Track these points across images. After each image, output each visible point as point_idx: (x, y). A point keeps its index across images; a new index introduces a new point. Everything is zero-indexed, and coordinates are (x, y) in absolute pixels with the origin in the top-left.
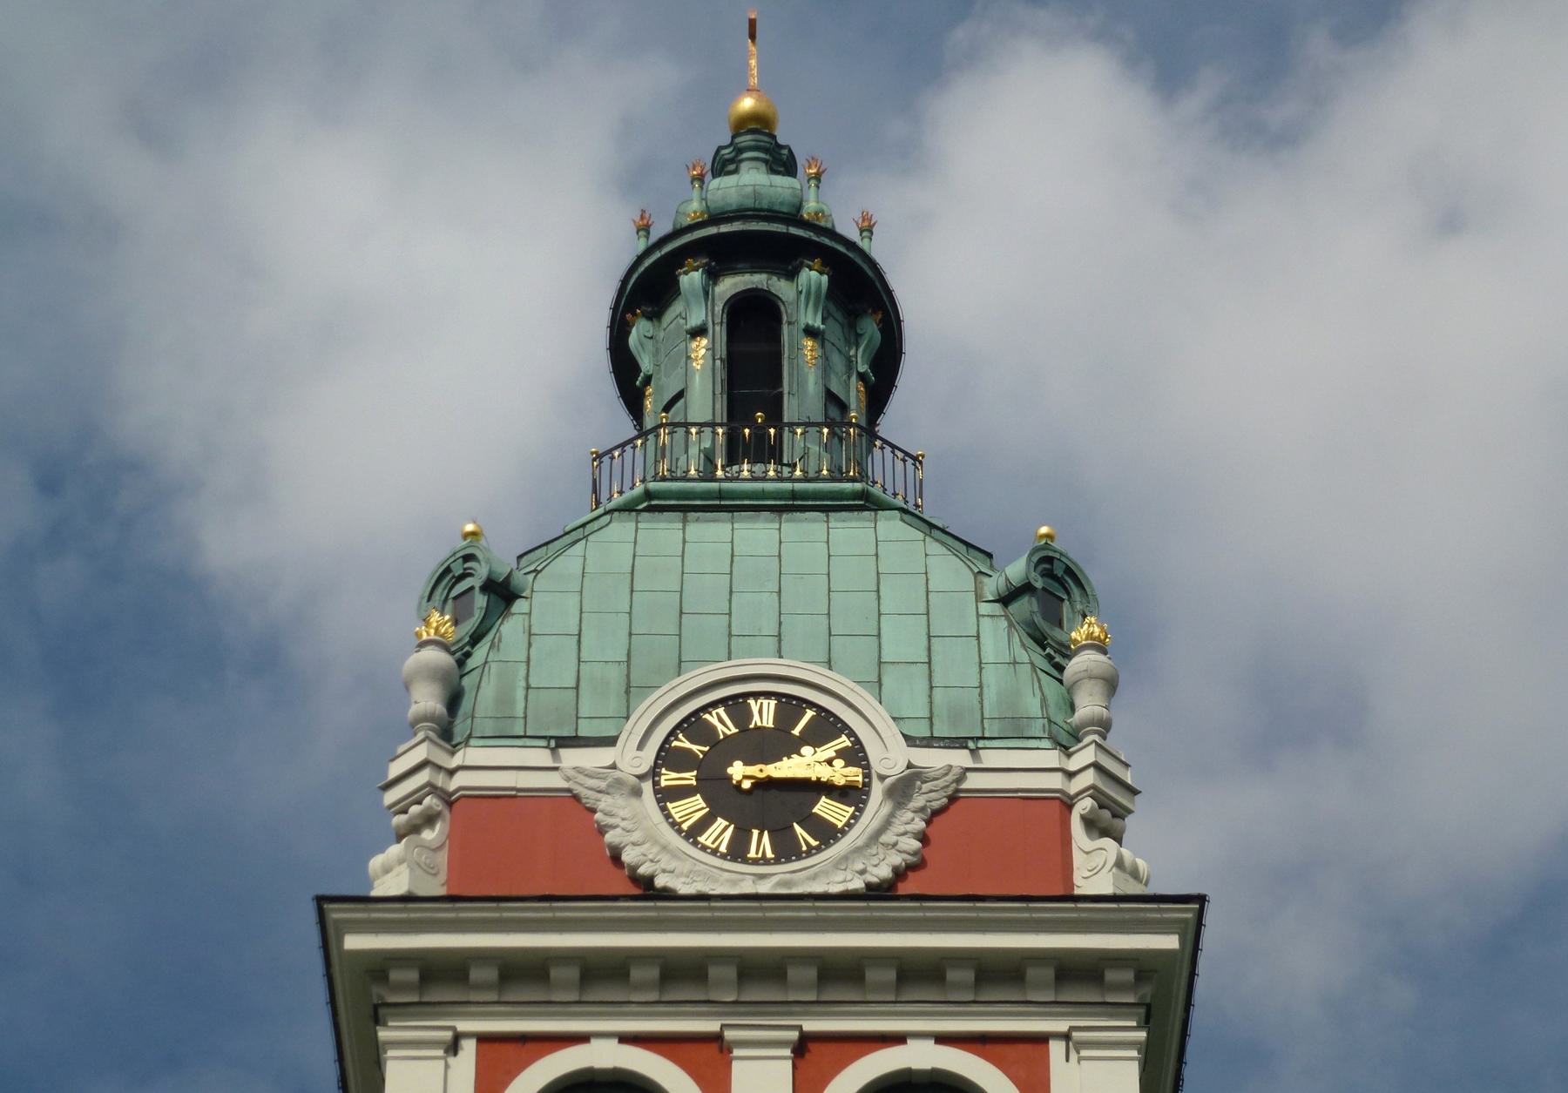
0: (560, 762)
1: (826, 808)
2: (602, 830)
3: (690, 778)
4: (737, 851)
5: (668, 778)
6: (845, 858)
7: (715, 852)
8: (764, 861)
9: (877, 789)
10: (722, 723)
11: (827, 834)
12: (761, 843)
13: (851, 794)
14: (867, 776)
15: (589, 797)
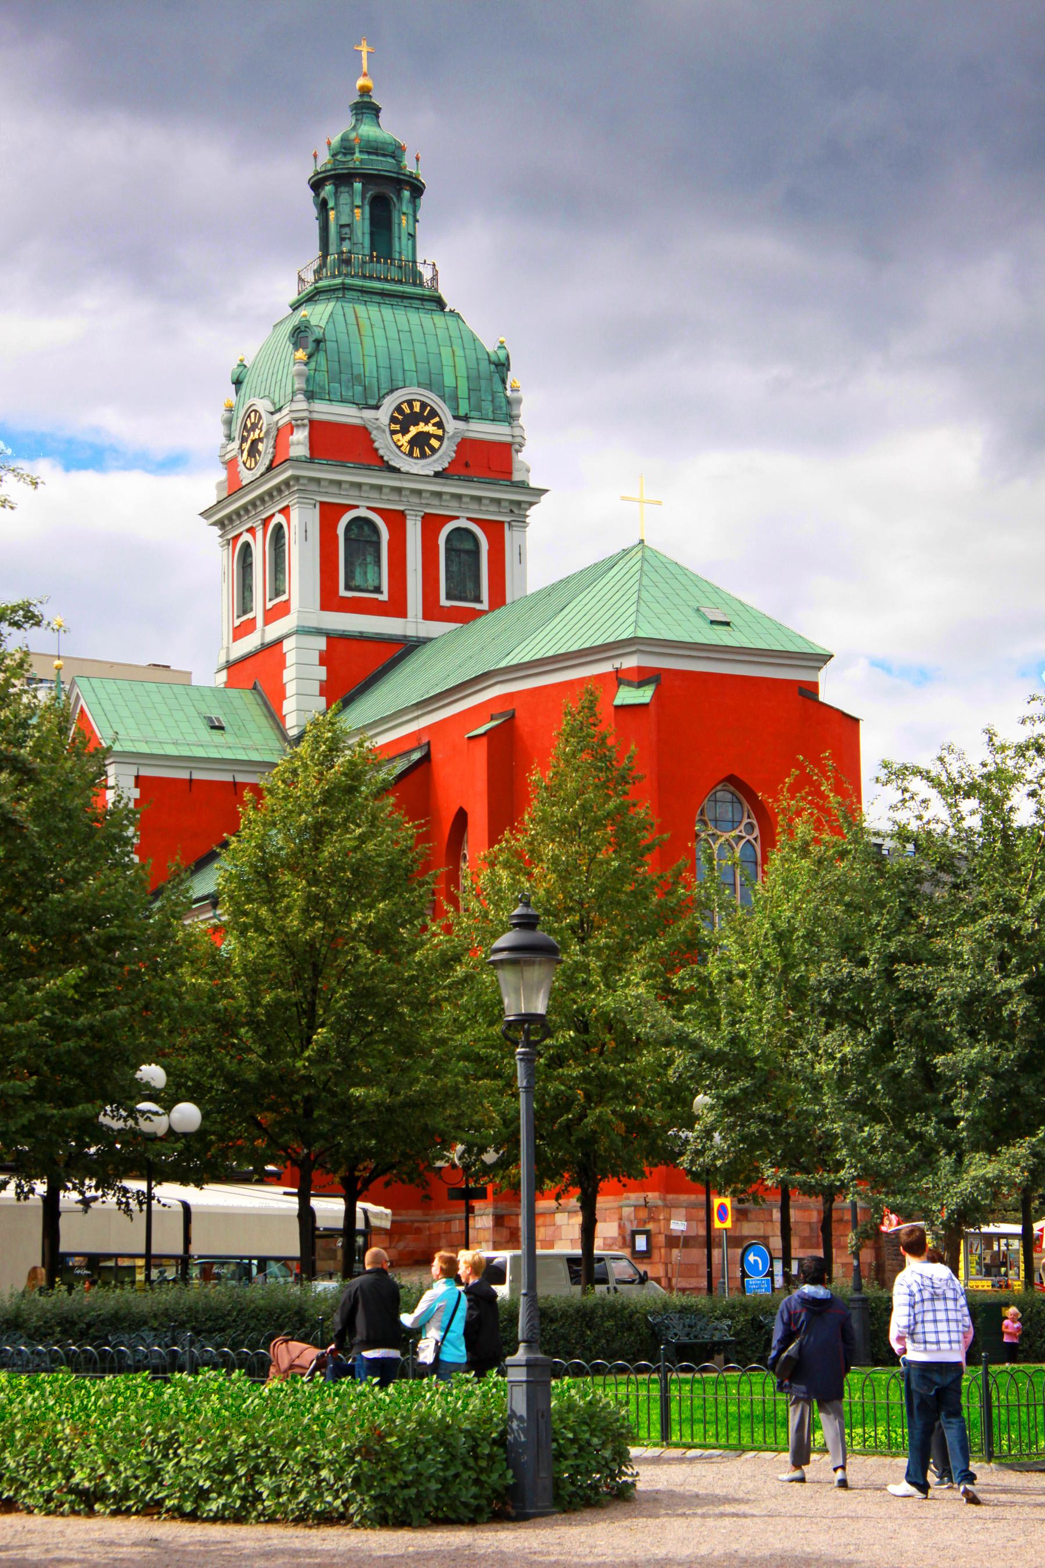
1: (434, 443)
2: (373, 442)
3: (398, 427)
4: (410, 454)
5: (394, 427)
6: (437, 460)
8: (417, 458)
9: (446, 435)
11: (434, 451)
12: (417, 452)
13: (440, 439)
14: (444, 431)
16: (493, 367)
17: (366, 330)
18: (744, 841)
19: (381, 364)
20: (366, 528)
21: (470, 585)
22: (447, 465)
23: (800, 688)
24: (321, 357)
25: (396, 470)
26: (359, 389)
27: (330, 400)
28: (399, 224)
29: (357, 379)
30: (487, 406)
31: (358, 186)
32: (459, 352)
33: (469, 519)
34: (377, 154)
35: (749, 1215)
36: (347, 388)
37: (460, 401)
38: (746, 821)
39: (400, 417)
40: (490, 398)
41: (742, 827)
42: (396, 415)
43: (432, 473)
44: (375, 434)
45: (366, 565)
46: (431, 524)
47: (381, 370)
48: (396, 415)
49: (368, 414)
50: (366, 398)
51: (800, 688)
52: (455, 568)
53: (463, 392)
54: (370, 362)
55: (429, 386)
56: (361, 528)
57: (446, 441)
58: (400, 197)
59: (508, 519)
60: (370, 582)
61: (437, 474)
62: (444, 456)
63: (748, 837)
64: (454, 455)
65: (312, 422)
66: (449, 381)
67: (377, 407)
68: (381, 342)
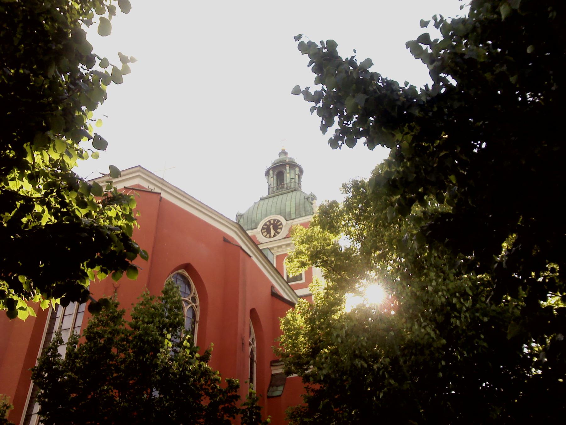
0: (85, 284)
3: (265, 230)
5: (263, 231)
10: (268, 224)
16: (306, 200)
28: (286, 177)
37: (292, 215)
49: (255, 230)
53: (293, 211)
55: (280, 214)
58: (286, 170)
66: (288, 210)
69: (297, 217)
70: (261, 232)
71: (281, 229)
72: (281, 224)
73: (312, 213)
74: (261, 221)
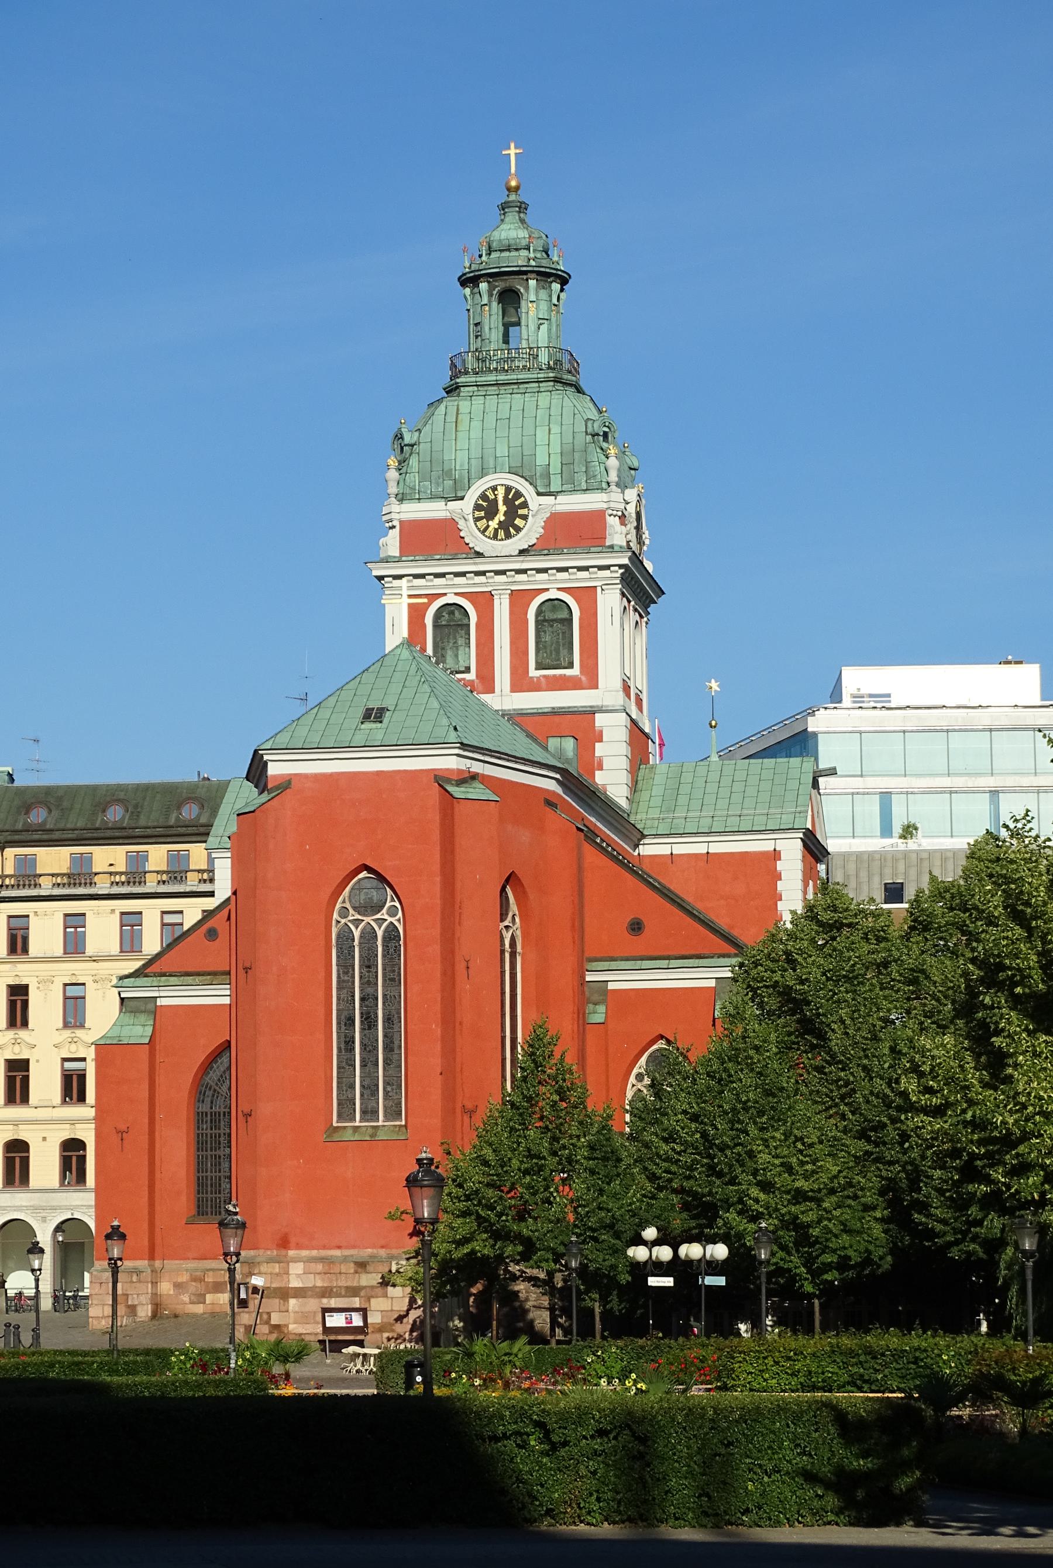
5: (477, 514)
7: (489, 538)
11: (518, 529)
13: (525, 518)
15: (457, 519)
16: (589, 437)
17: (463, 426)
18: (363, 924)
19: (473, 456)
20: (457, 613)
21: (564, 652)
22: (534, 541)
23: (436, 776)
24: (414, 461)
25: (479, 555)
26: (449, 483)
27: (419, 499)
29: (447, 474)
30: (582, 480)
31: (483, 286)
32: (556, 429)
33: (559, 589)
34: (509, 250)
35: (369, 1268)
36: (438, 484)
38: (388, 904)
39: (485, 504)
40: (584, 469)
41: (384, 911)
42: (481, 502)
43: (517, 552)
44: (461, 524)
45: (457, 648)
46: (519, 599)
47: (473, 461)
48: (481, 502)
49: (453, 505)
50: (456, 491)
51: (436, 776)
52: (547, 638)
53: (555, 467)
54: (462, 457)
56: (452, 613)
57: (530, 517)
58: (527, 288)
59: (600, 583)
60: (461, 663)
61: (522, 552)
62: (531, 531)
63: (390, 919)
64: (542, 531)
65: (401, 522)
66: (541, 460)
67: (462, 498)
68: (475, 434)
69: (565, 488)
70: (470, 518)
71: (525, 518)
72: (525, 505)
73: (604, 485)
74: (469, 488)
